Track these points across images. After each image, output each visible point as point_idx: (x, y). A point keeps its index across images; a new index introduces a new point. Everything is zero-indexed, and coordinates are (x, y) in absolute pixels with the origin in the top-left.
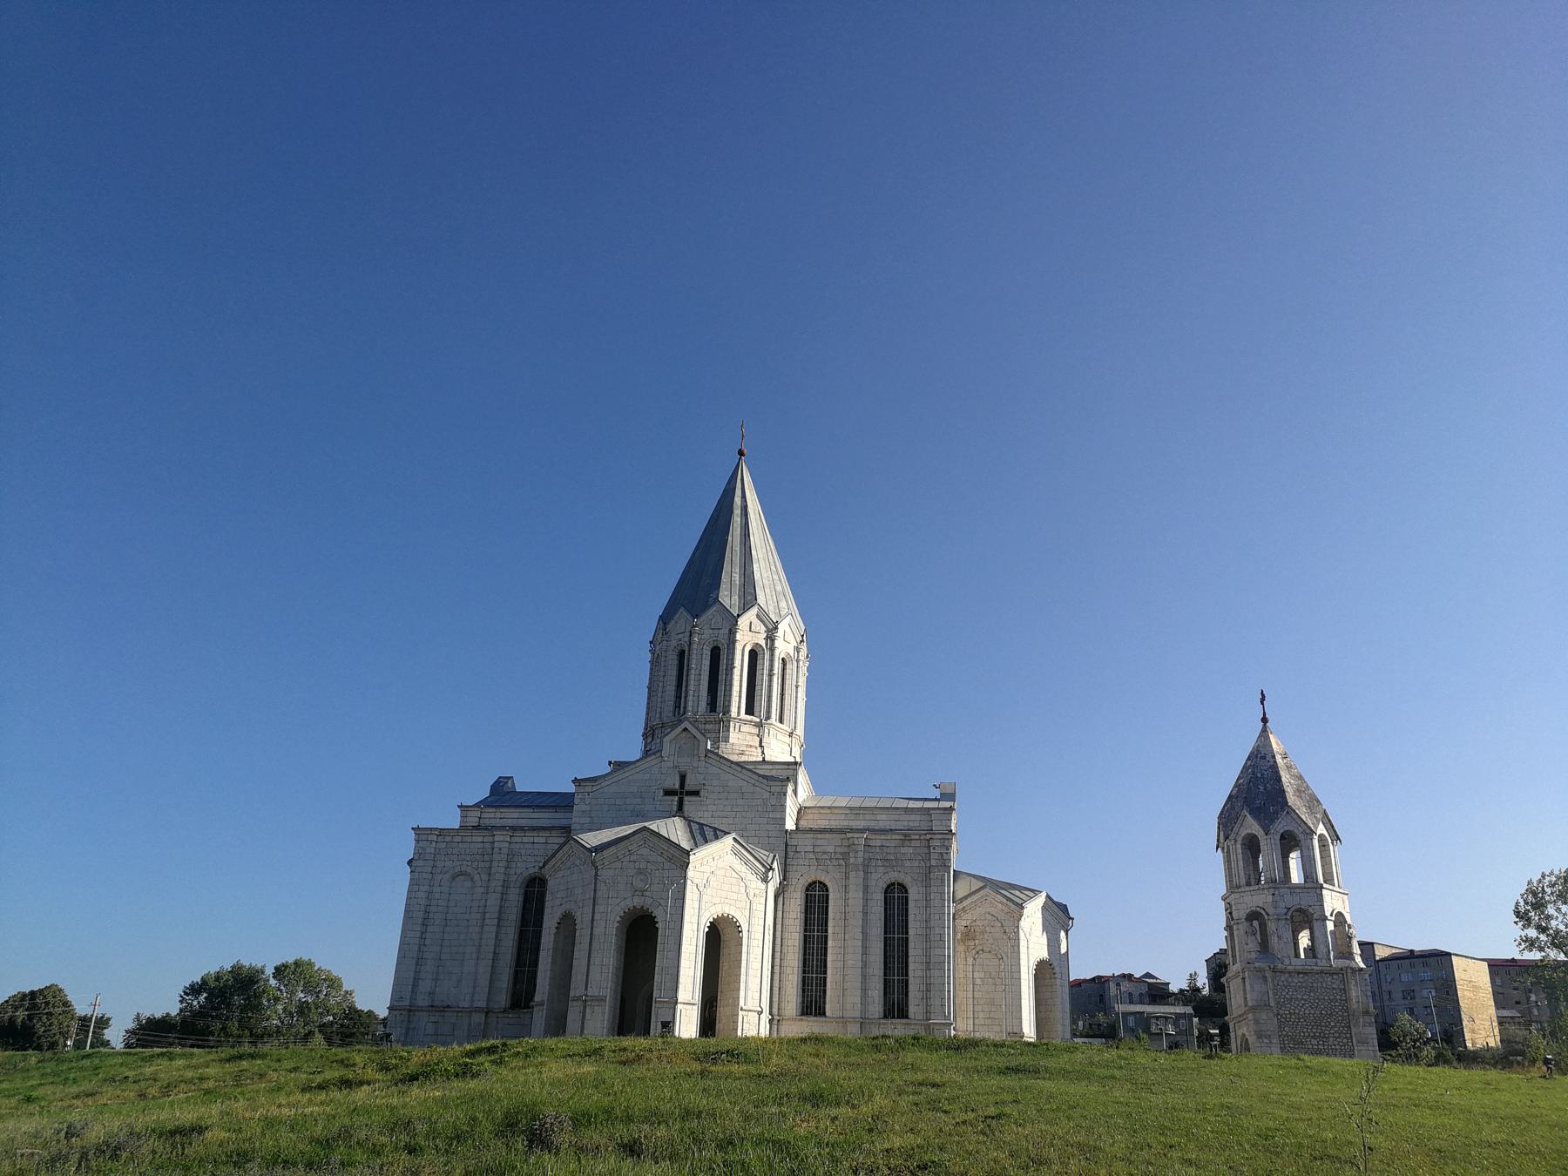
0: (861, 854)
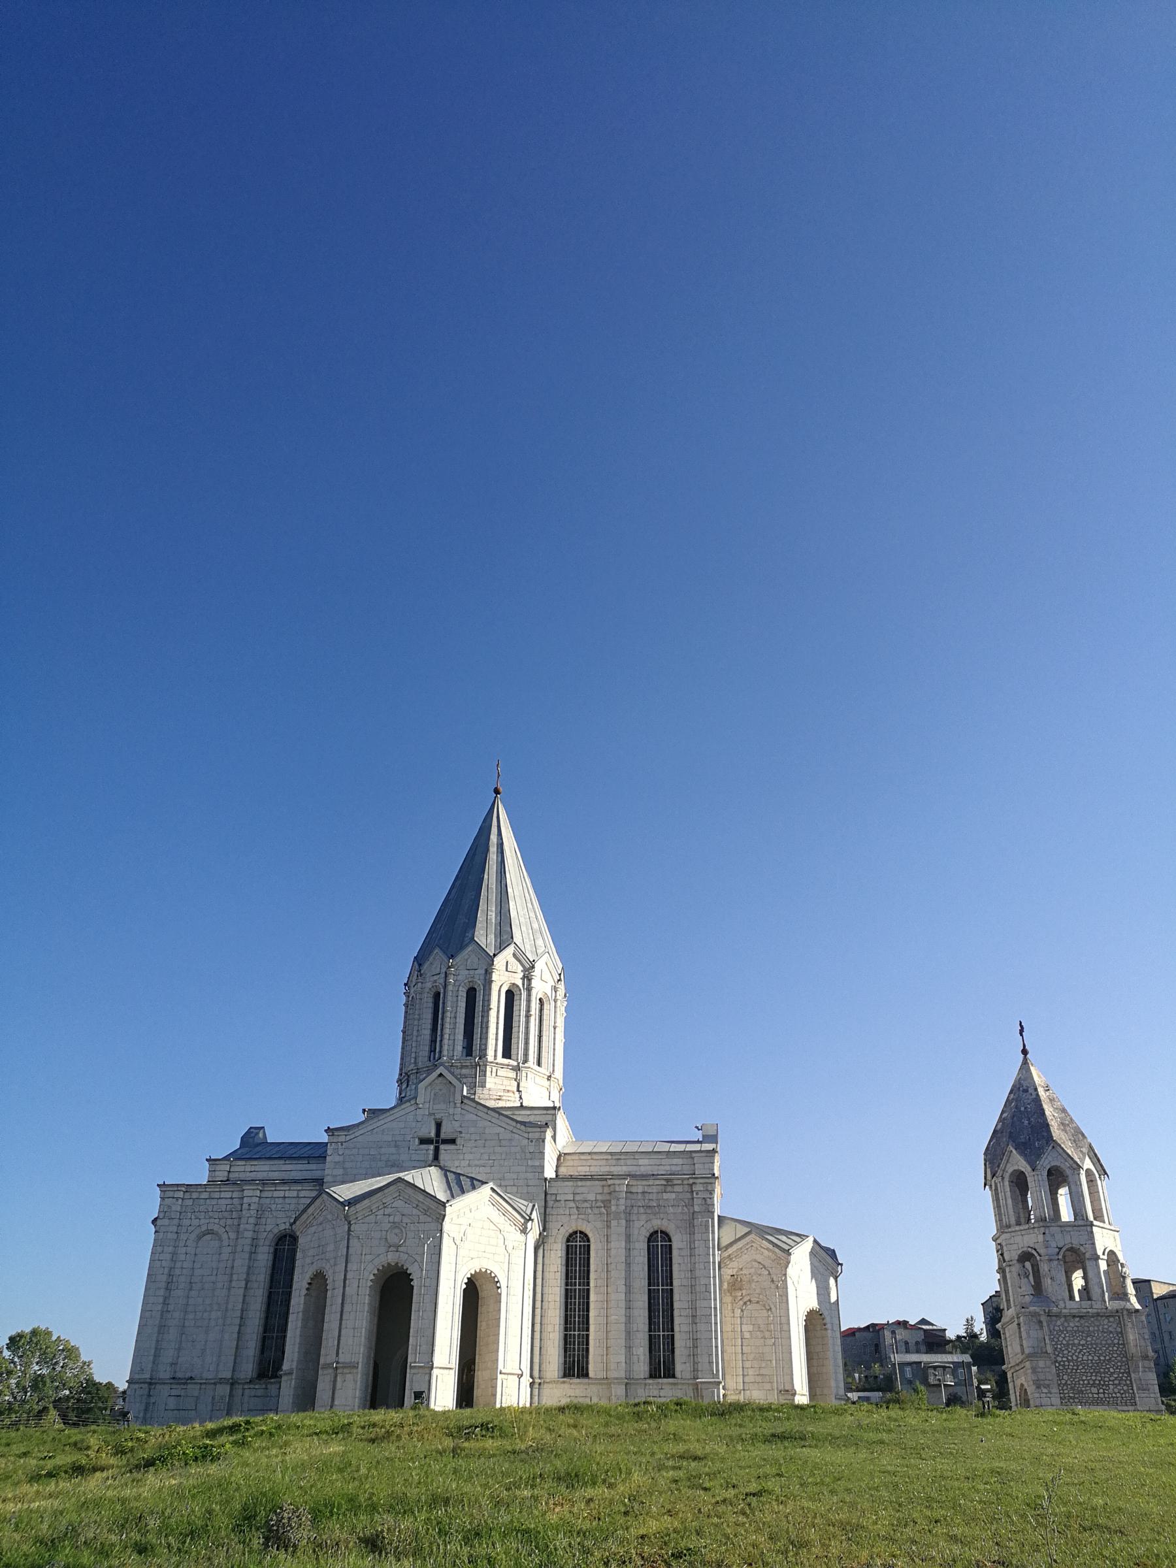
0: (622, 1201)
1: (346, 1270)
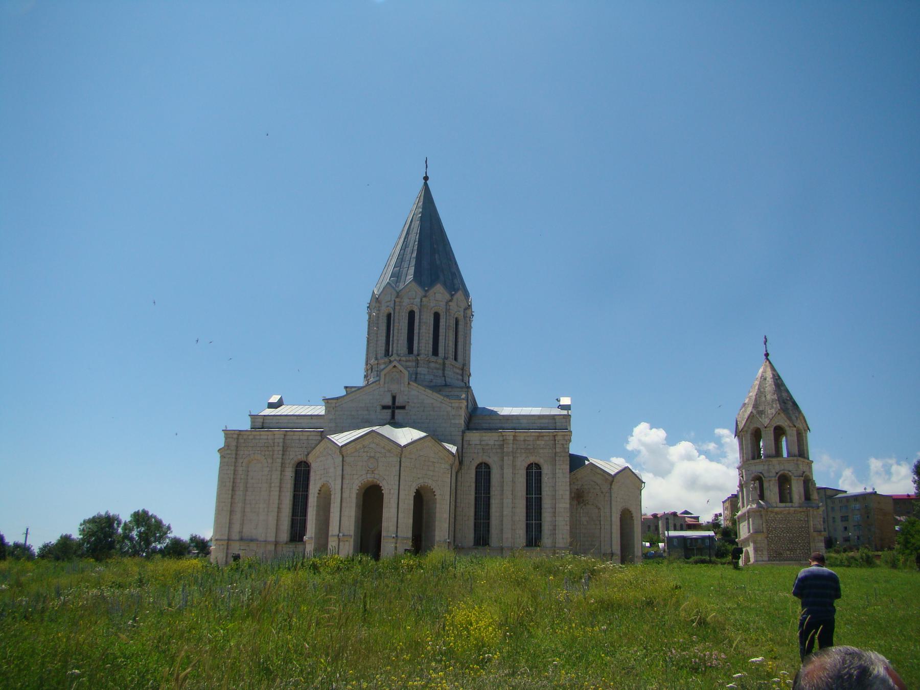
0: (511, 445)
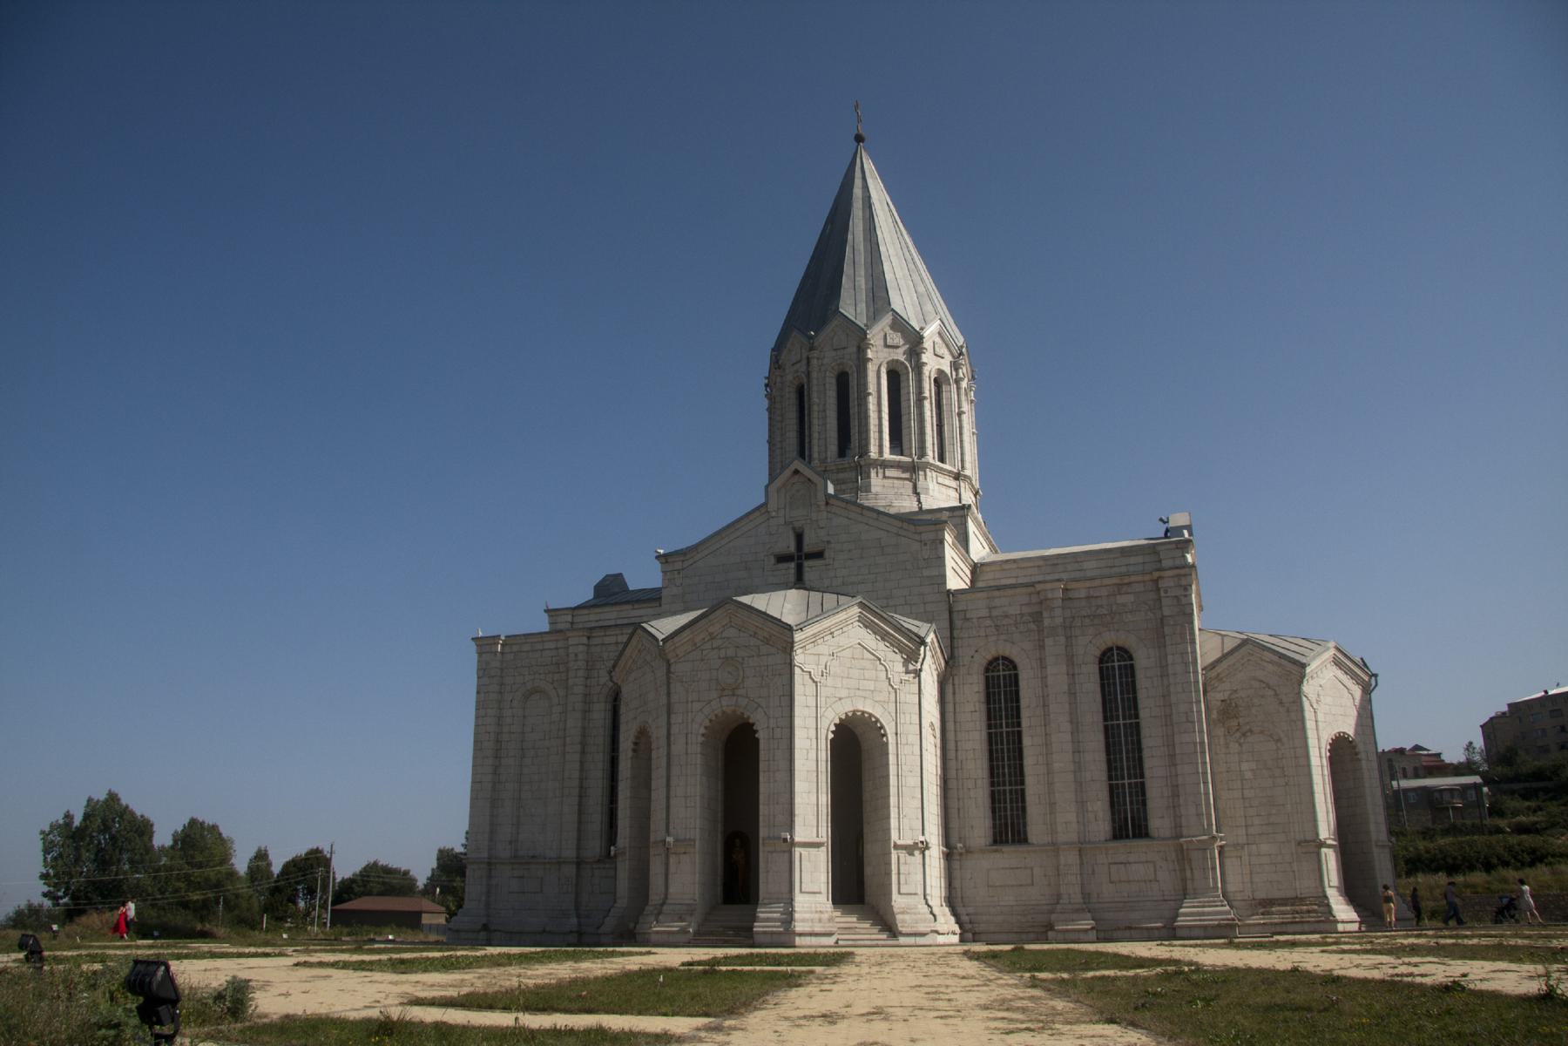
0: (1058, 612)
1: (669, 724)
